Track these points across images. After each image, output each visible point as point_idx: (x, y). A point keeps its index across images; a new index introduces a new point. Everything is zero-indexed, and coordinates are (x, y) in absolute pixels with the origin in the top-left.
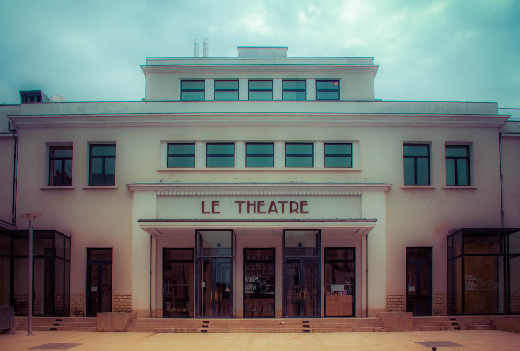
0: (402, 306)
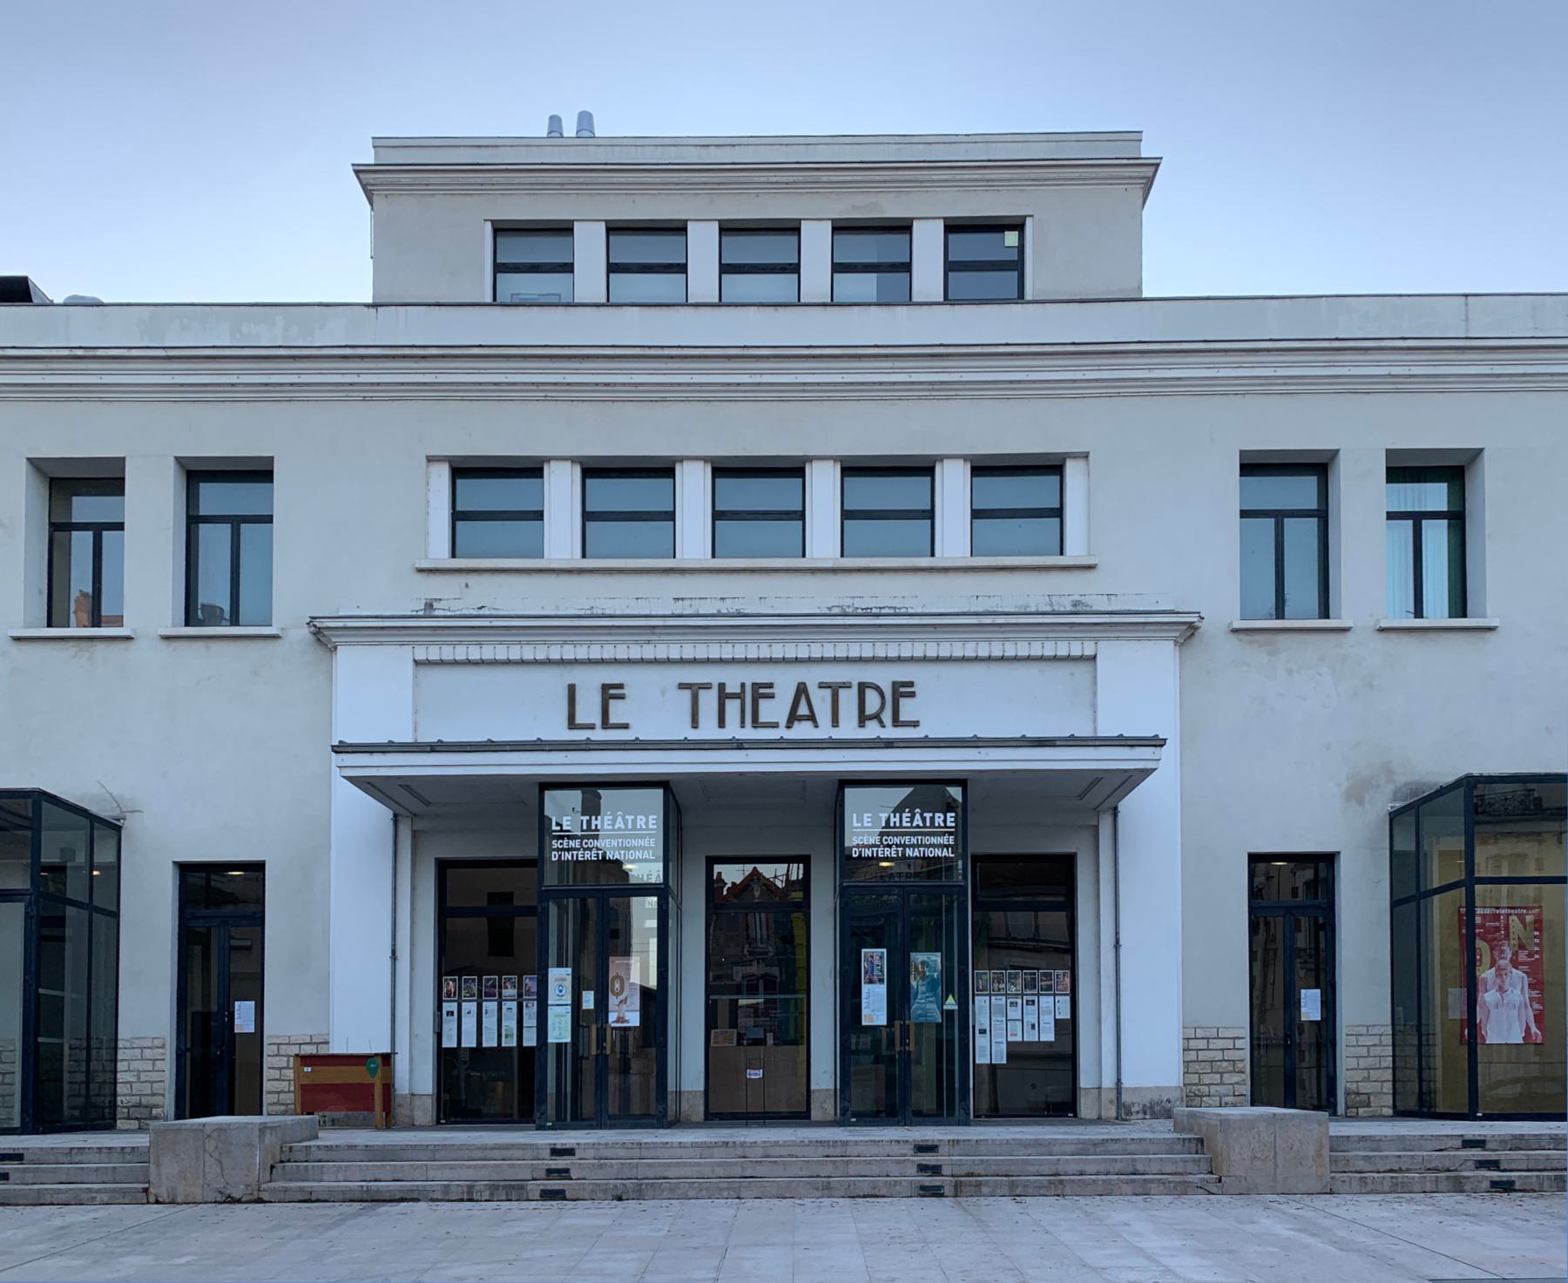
0: (1236, 1078)
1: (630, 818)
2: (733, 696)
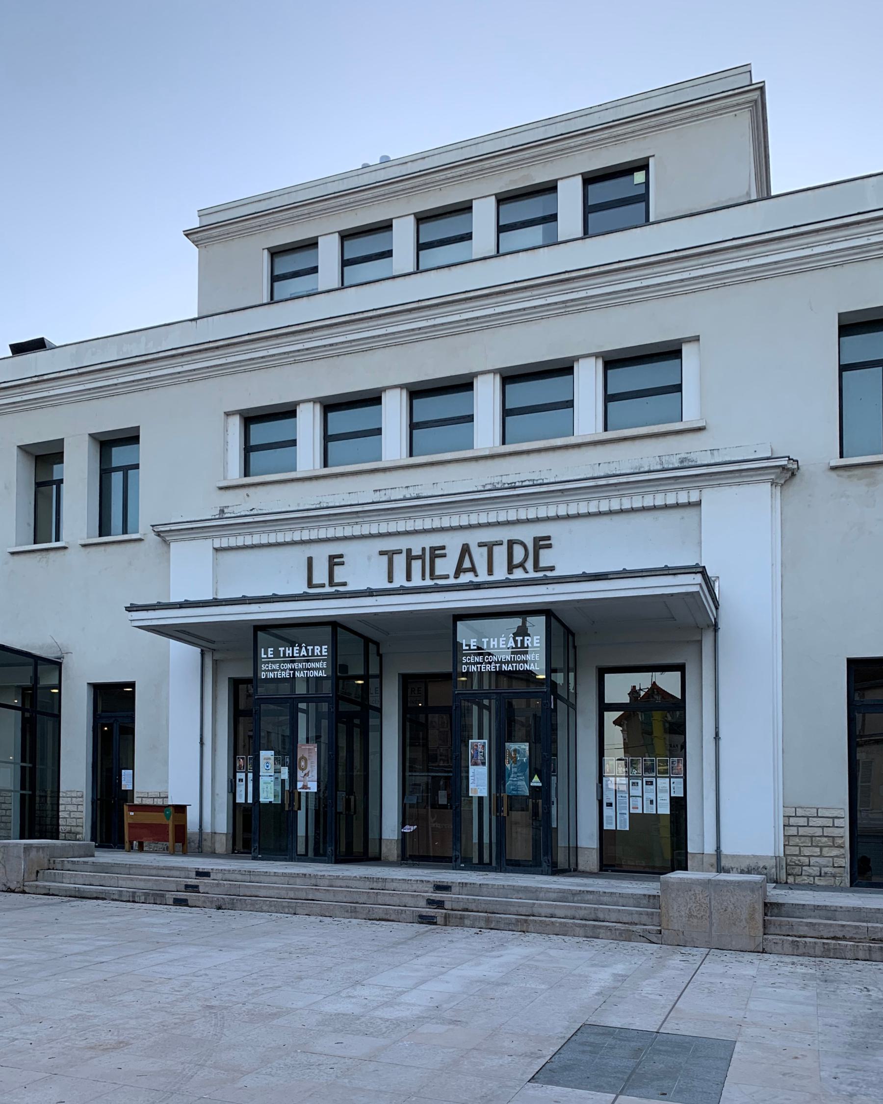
0: (835, 852)
1: (310, 648)
2: (417, 558)
